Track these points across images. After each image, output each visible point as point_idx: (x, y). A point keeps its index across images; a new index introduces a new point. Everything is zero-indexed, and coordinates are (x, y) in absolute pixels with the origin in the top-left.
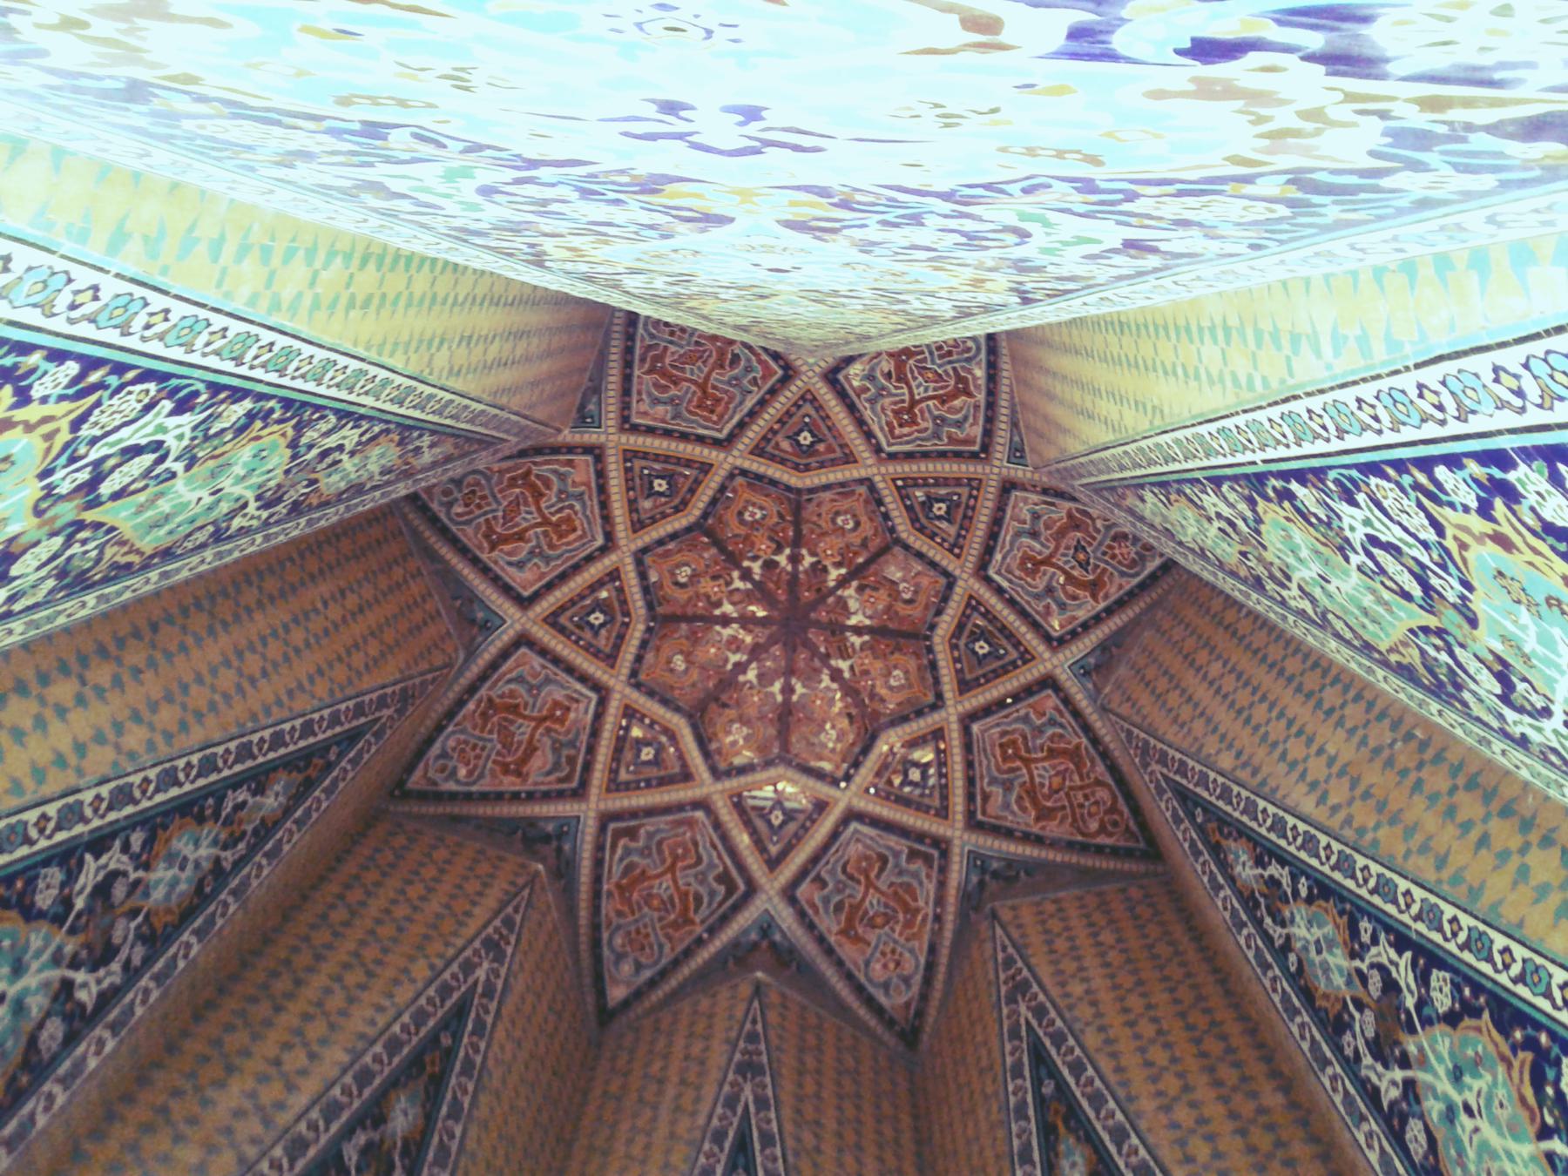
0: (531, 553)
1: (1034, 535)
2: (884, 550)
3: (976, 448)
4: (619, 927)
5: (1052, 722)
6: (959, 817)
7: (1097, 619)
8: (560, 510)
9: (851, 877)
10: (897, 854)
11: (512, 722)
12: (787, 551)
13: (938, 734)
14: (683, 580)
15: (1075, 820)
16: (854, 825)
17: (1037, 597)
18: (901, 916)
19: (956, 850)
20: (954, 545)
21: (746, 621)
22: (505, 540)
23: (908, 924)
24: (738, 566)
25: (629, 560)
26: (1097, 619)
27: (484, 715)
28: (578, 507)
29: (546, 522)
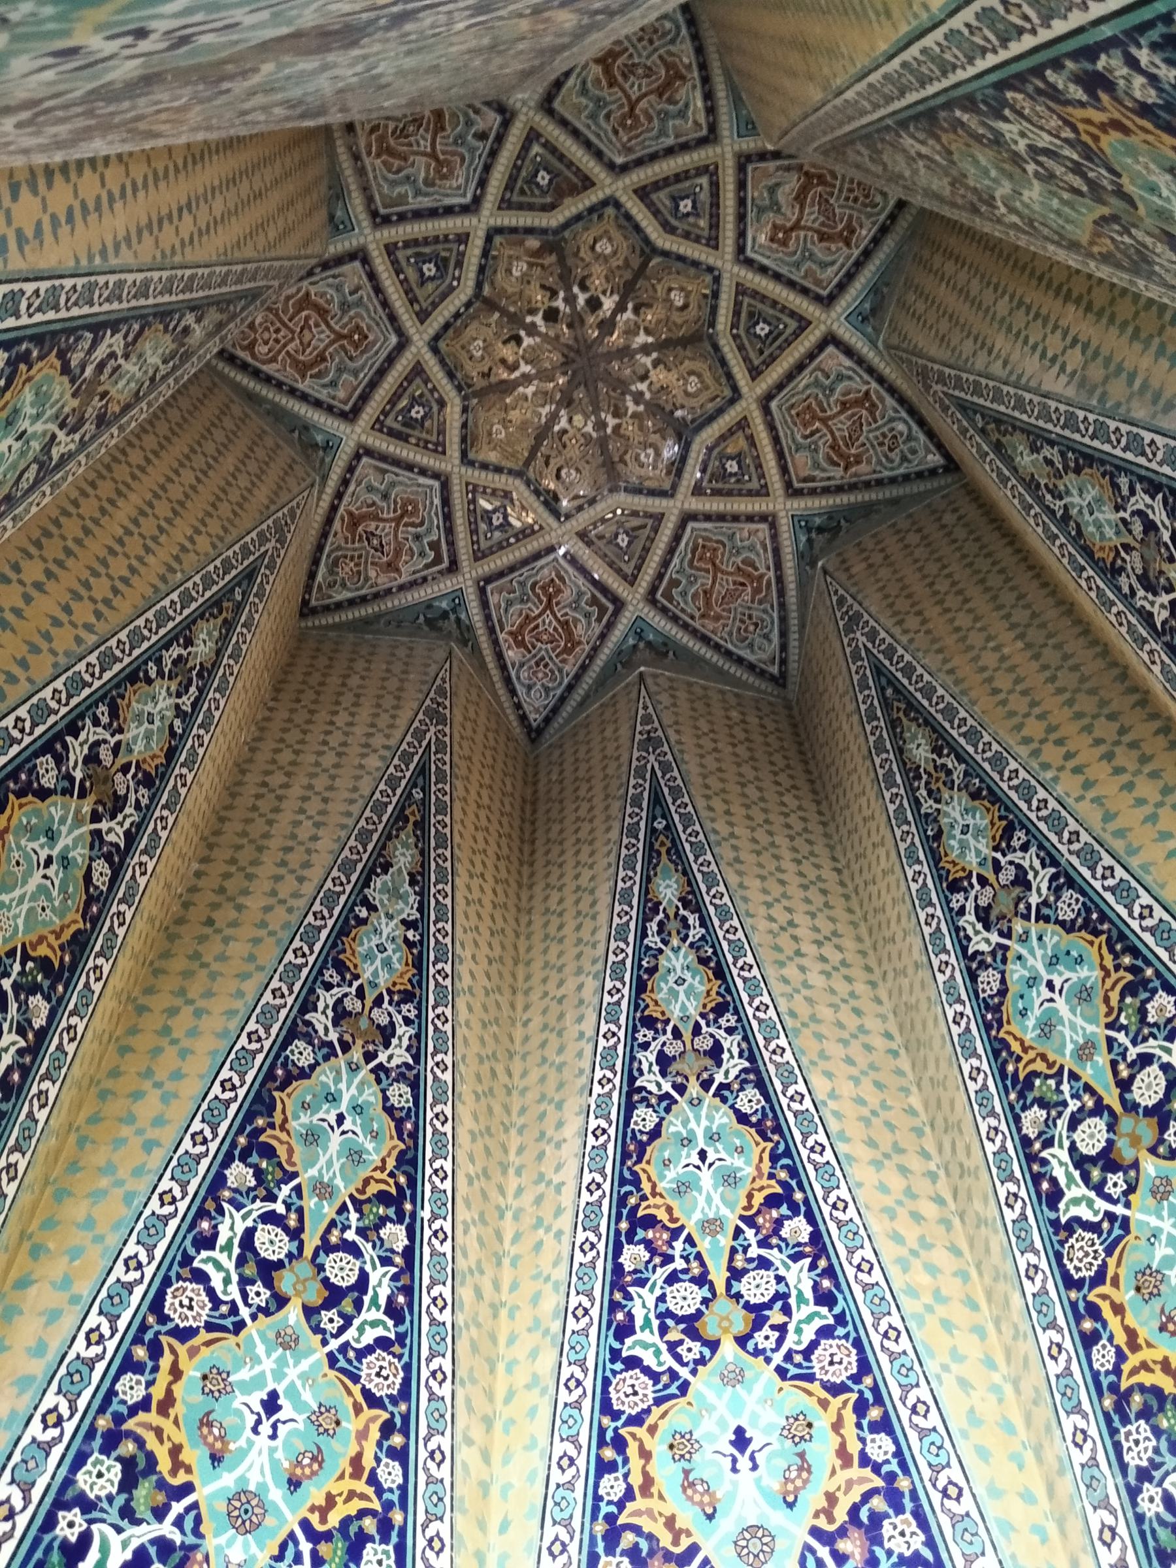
0: (832, 390)
1: (417, 537)
2: (527, 463)
3: (489, 588)
4: (673, 41)
5: (333, 384)
6: (375, 253)
7: (339, 495)
8: (812, 434)
9: (453, 154)
10: (418, 193)
11: (823, 224)
12: (609, 430)
13: (423, 316)
14: (693, 379)
15: (277, 315)
16: (468, 199)
17: (393, 484)
18: (392, 142)
19: (365, 224)
20: (474, 491)
21: (625, 353)
22: (858, 403)
23: (382, 139)
24: (647, 404)
25: (744, 390)
26: (339, 495)
27: (853, 232)
28: (798, 437)
29: (824, 421)
